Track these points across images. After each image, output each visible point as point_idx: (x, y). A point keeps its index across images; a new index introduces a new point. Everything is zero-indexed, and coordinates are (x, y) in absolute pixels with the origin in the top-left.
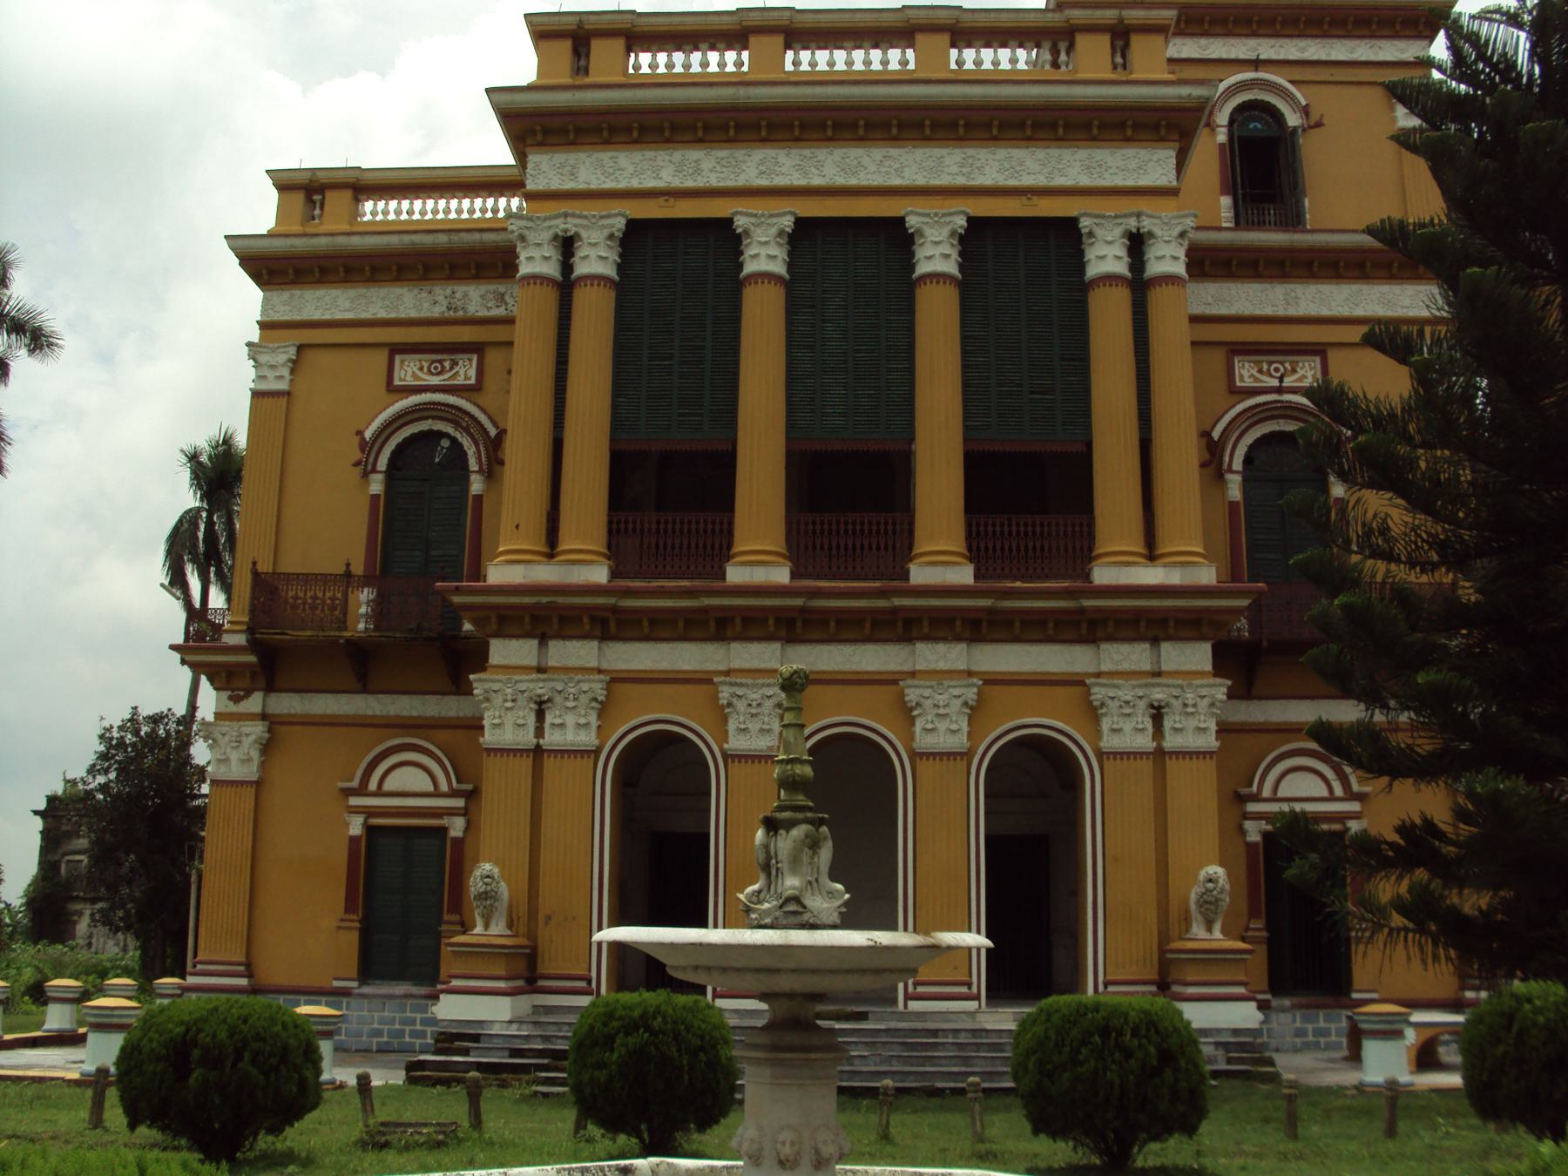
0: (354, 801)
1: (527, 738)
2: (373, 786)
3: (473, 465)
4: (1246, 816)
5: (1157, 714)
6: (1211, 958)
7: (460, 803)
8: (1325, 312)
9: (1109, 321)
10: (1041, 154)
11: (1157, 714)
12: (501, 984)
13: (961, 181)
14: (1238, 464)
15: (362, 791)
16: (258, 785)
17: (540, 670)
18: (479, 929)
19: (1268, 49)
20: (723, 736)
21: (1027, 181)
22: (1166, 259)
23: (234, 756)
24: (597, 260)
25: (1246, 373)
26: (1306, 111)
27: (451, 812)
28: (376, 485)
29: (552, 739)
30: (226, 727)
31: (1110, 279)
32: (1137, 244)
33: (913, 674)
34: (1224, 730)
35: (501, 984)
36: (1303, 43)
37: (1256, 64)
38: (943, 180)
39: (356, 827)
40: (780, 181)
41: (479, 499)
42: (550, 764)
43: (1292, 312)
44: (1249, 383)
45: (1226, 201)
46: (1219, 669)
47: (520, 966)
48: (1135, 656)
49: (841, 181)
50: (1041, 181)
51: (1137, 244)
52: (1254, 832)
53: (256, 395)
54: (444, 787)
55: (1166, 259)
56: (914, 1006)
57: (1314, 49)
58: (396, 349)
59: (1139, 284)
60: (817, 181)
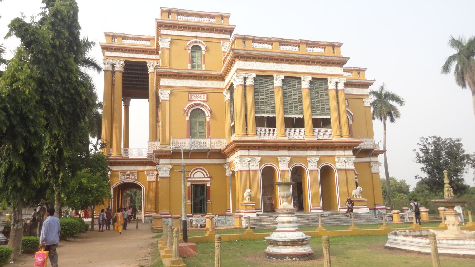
0: (188, 180)
1: (247, 168)
2: (192, 177)
3: (207, 115)
6: (359, 201)
7: (209, 179)
9: (332, 96)
12: (254, 211)
15: (190, 178)
16: (170, 178)
17: (249, 156)
18: (245, 201)
20: (279, 167)
22: (341, 87)
24: (250, 82)
27: (208, 181)
28: (188, 119)
29: (252, 168)
31: (333, 89)
34: (355, 163)
35: (254, 211)
39: (189, 185)
41: (208, 122)
42: (251, 172)
46: (354, 154)
51: (337, 83)
54: (206, 176)
55: (341, 87)
56: (312, 211)
58: (190, 93)
59: (337, 91)
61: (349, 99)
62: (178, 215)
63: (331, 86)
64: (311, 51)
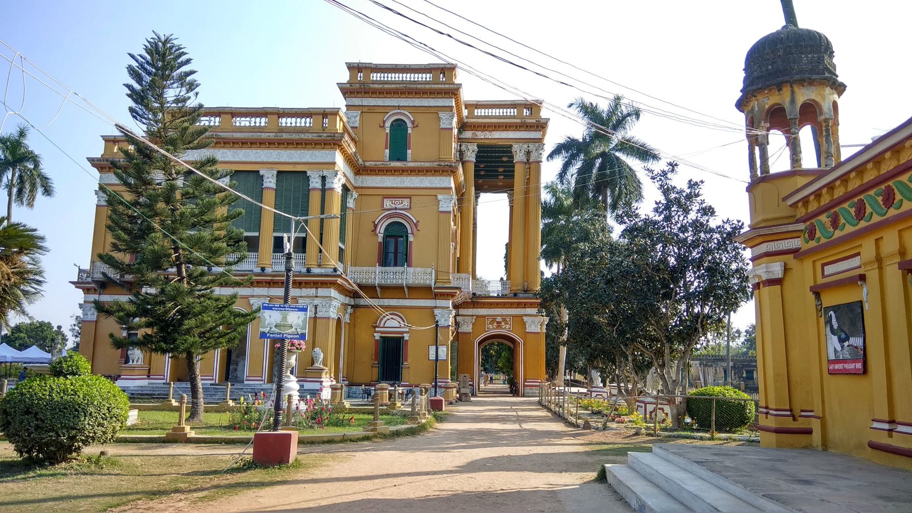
4: (375, 332)
5: (316, 307)
8: (412, 186)
10: (299, 152)
11: (316, 307)
13: (276, 160)
14: (382, 231)
19: (403, 102)
21: (294, 160)
23: (89, 313)
25: (388, 203)
26: (413, 122)
30: (87, 305)
32: (324, 178)
33: (253, 296)
36: (415, 100)
37: (399, 107)
38: (271, 160)
40: (227, 159)
43: (402, 186)
44: (389, 207)
45: (387, 151)
47: (146, 372)
48: (312, 291)
49: (244, 160)
50: (298, 160)
51: (324, 178)
52: (377, 336)
53: (98, 206)
57: (417, 102)
59: (324, 190)
60: (237, 160)
61: (413, 198)
62: (316, 386)
63: (315, 183)
64: (289, 125)
